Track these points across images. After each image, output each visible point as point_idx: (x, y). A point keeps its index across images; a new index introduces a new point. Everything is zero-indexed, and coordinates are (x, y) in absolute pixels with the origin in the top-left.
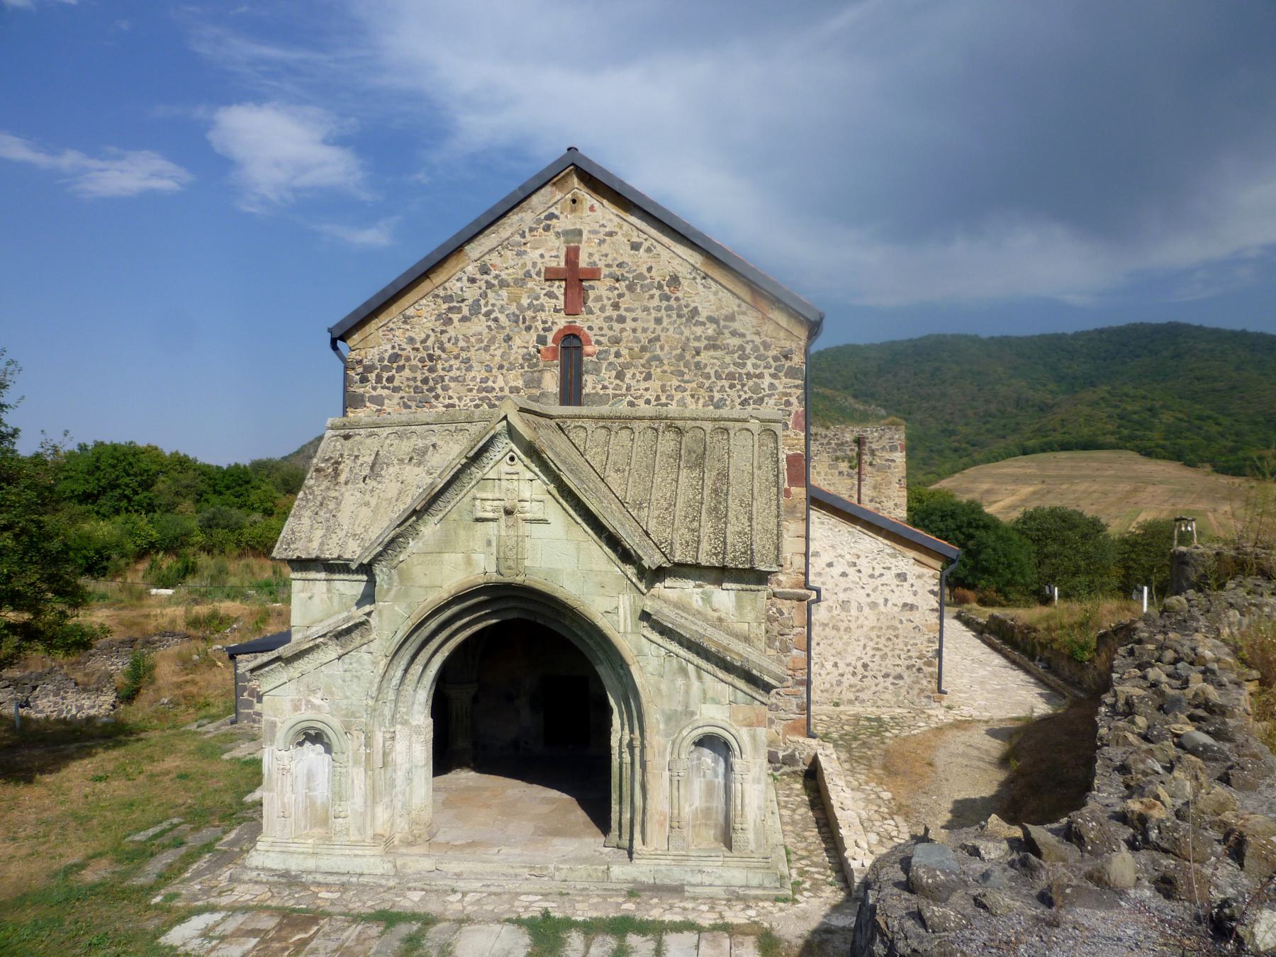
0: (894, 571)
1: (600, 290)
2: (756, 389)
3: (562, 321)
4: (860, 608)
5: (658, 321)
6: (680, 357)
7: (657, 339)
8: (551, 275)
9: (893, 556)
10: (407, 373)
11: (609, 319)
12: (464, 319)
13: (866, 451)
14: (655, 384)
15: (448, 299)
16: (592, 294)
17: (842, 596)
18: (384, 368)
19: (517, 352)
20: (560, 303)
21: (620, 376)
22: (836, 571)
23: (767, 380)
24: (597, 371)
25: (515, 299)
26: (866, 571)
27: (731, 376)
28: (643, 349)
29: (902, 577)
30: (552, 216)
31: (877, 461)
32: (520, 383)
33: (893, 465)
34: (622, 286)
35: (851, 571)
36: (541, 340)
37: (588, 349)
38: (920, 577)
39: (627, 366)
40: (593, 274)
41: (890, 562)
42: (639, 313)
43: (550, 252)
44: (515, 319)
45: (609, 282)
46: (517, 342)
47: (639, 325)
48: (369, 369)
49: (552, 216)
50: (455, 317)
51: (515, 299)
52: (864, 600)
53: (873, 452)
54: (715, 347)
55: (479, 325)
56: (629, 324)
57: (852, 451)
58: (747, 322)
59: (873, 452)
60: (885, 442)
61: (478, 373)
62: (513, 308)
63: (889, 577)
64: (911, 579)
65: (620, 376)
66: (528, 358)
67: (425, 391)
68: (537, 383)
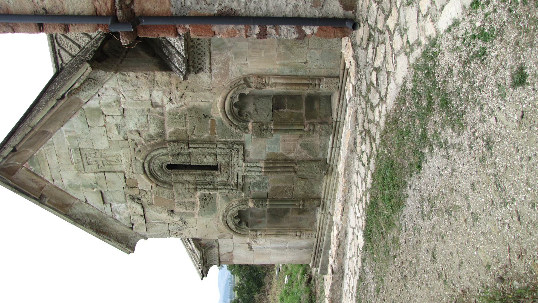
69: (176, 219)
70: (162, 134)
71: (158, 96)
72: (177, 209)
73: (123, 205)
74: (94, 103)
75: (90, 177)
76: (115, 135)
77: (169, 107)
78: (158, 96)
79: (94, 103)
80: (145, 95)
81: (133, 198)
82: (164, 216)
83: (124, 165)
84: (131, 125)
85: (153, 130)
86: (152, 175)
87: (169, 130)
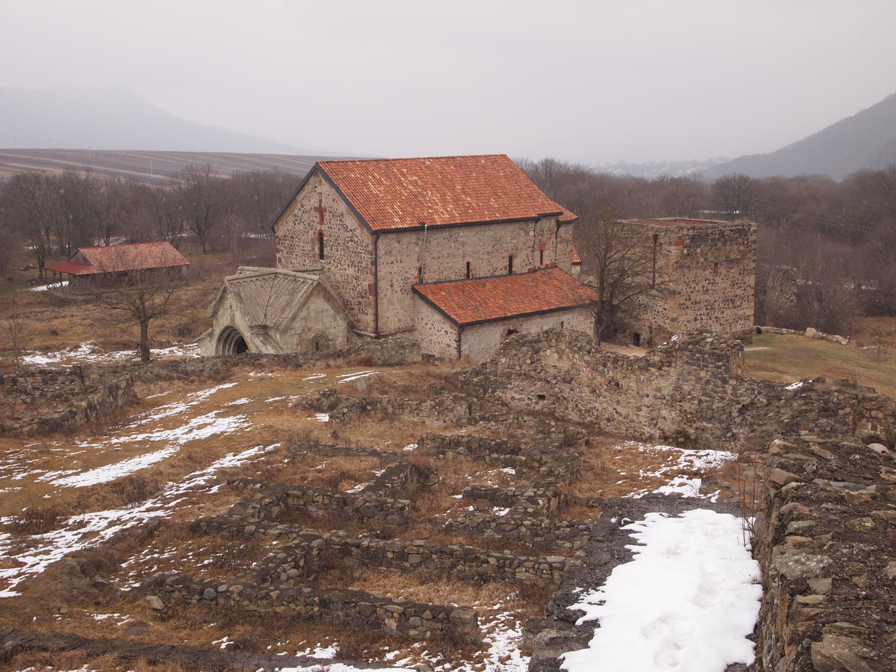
0: (444, 330)
1: (327, 216)
2: (361, 259)
3: (319, 227)
4: (435, 344)
5: (339, 229)
6: (344, 243)
7: (339, 236)
8: (316, 209)
9: (444, 323)
10: (287, 242)
11: (329, 227)
12: (299, 224)
13: (658, 244)
14: (339, 253)
15: (295, 215)
16: (325, 217)
17: (430, 338)
18: (284, 240)
19: (310, 237)
20: (318, 220)
21: (331, 249)
22: (429, 326)
23: (363, 255)
24: (326, 247)
25: (309, 218)
26: (437, 328)
27: (355, 252)
28: (336, 240)
29: (446, 332)
30: (316, 187)
31: (663, 252)
32: (310, 249)
33: (670, 254)
34: (331, 215)
35: (432, 327)
36: (315, 233)
37: (325, 238)
38: (451, 333)
39: (333, 245)
40: (325, 210)
41: (443, 326)
42: (335, 226)
43: (314, 202)
44: (309, 225)
45: (328, 213)
46: (310, 234)
47: (335, 230)
48: (280, 239)
49: (316, 187)
50: (297, 223)
51: (309, 218)
52: (436, 340)
53: (661, 244)
54: (351, 241)
55: (301, 227)
56: (333, 230)
57: (650, 244)
58: (358, 232)
59: (661, 244)
60: (666, 239)
61: (302, 244)
62: (308, 221)
63: (443, 332)
64: (449, 334)
65: (331, 249)
66: (312, 240)
67: (291, 249)
68: (313, 249)
69: (295, 347)
70: (329, 340)
71: (340, 339)
72: (299, 347)
73: (299, 325)
74: (338, 318)
75: (313, 315)
76: (328, 325)
77: (337, 342)
78: (340, 339)
79: (338, 318)
80: (340, 334)
81: (303, 330)
82: (295, 342)
83: (317, 327)
84: (331, 330)
85: (330, 337)
86: (315, 337)
87: (330, 343)
